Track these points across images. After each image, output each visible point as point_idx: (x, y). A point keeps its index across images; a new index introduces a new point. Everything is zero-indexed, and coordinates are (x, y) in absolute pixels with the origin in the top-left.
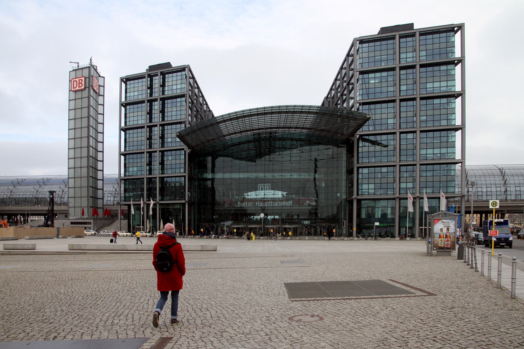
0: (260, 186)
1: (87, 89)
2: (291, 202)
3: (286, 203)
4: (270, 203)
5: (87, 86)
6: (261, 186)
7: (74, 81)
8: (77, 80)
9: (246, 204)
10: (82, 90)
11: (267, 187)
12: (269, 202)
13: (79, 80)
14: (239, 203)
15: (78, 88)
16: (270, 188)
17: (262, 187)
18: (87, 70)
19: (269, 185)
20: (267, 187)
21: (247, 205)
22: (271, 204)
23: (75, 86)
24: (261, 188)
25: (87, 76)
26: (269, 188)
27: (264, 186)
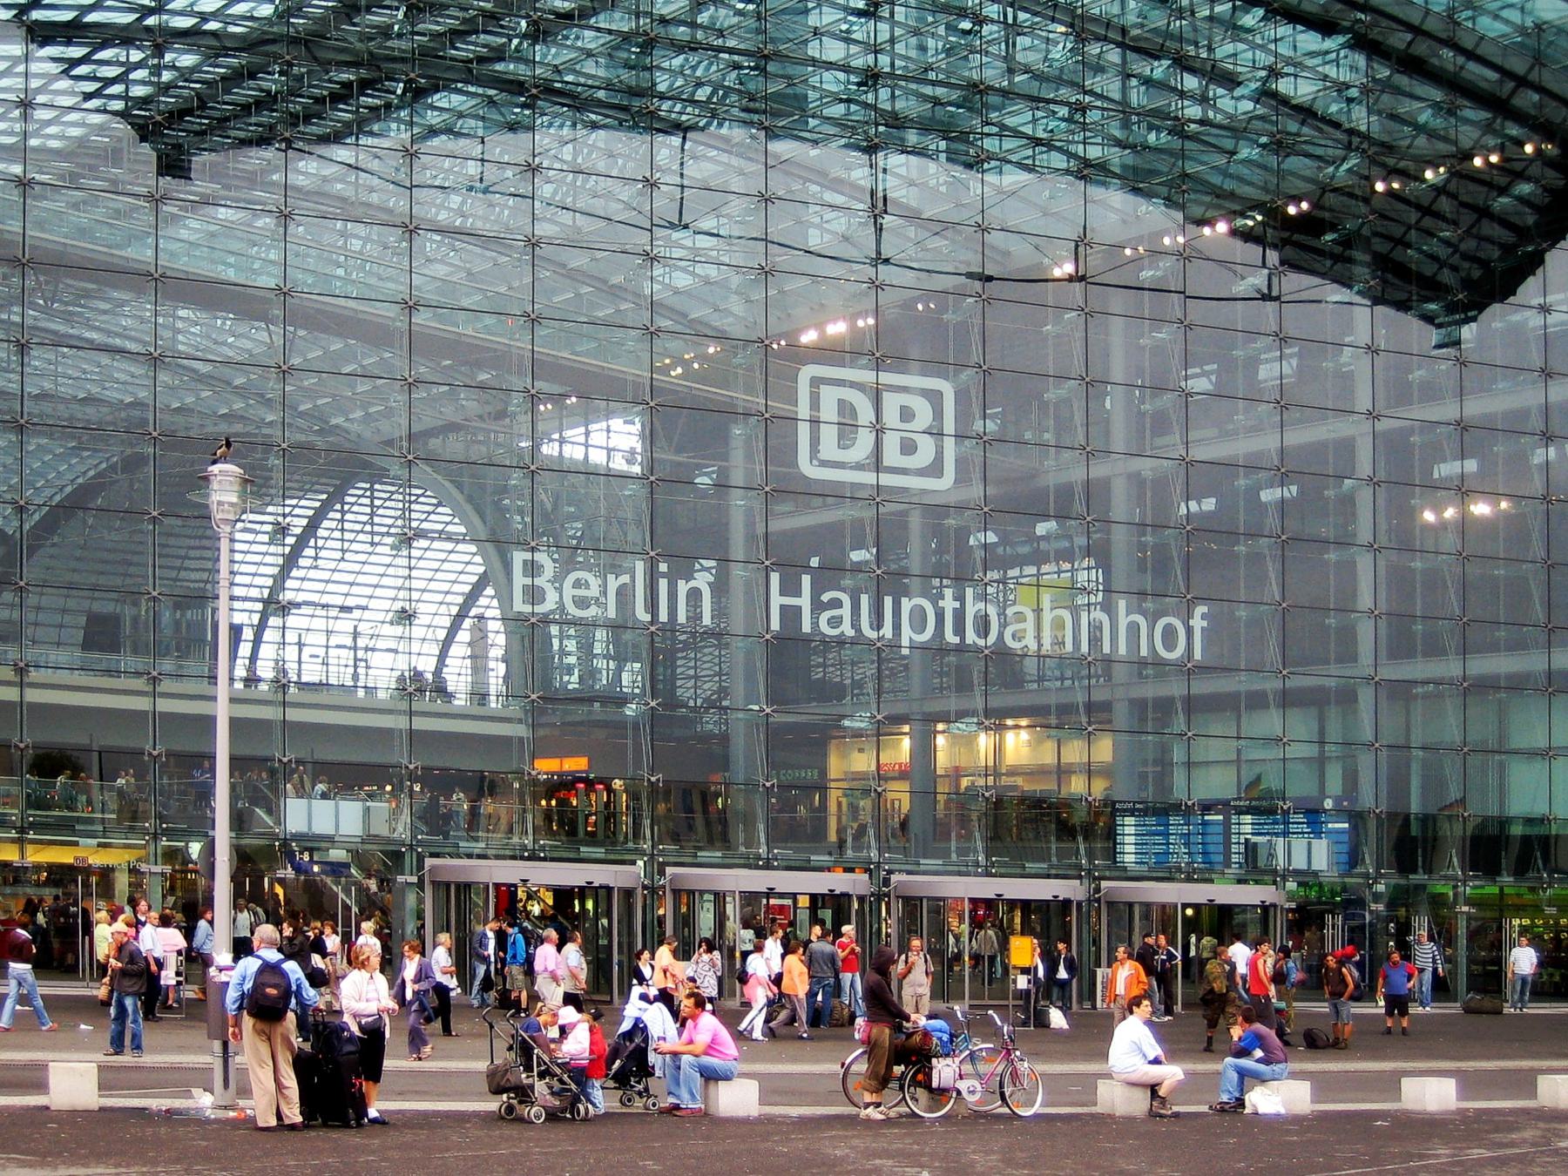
0: (816, 382)
2: (1198, 623)
3: (1134, 629)
4: (949, 604)
6: (829, 396)
11: (906, 414)
12: (936, 598)
14: (532, 569)
16: (949, 426)
17: (845, 408)
19: (935, 398)
20: (906, 414)
21: (652, 606)
22: (960, 616)
24: (829, 412)
26: (936, 433)
27: (877, 396)
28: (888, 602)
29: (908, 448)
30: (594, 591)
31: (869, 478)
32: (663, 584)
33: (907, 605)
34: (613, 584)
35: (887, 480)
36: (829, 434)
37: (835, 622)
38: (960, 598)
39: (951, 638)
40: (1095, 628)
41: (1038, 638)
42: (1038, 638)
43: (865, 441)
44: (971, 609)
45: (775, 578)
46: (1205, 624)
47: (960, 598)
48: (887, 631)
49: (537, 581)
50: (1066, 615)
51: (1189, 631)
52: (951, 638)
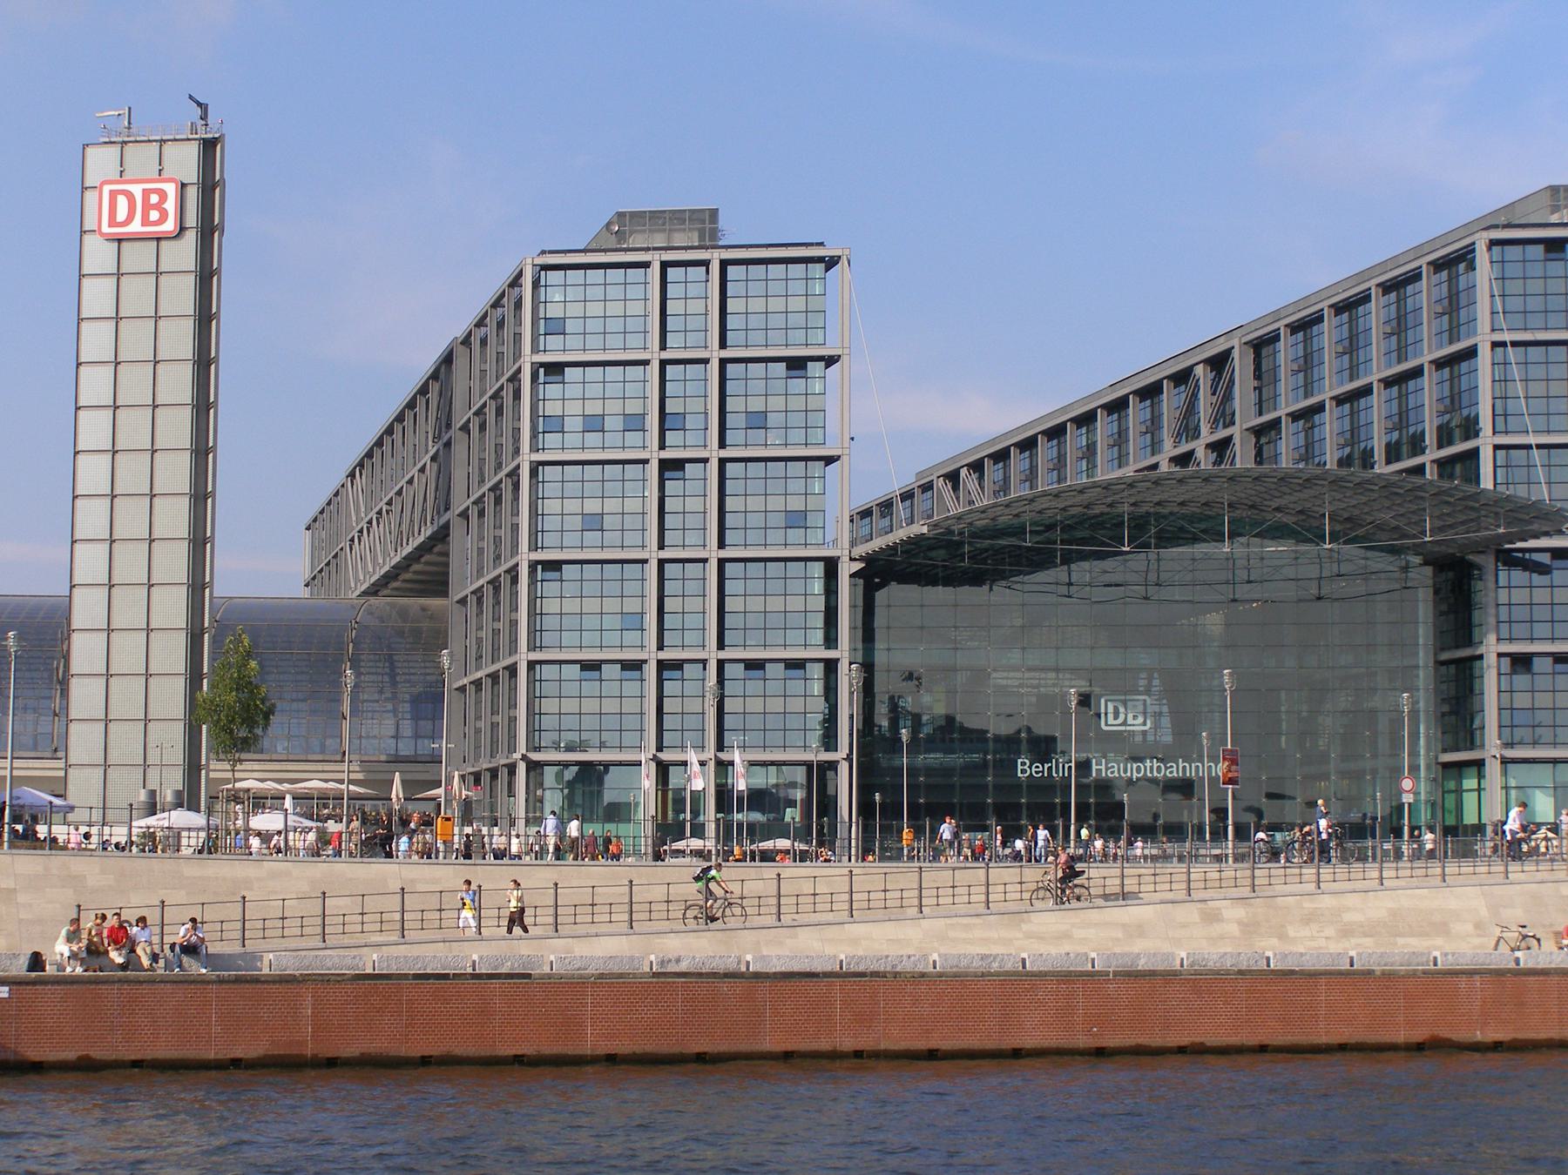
1: (191, 237)
4: (1148, 764)
5: (192, 219)
7: (113, 194)
8: (137, 190)
9: (1050, 769)
10: (158, 239)
13: (146, 193)
14: (1023, 764)
15: (136, 227)
17: (1116, 709)
18: (192, 152)
21: (1057, 772)
22: (1152, 768)
23: (122, 215)
25: (191, 174)
28: (1129, 765)
29: (1135, 717)
30: (1041, 769)
31: (1123, 728)
32: (1061, 765)
34: (1046, 766)
35: (1128, 728)
36: (1111, 716)
37: (1112, 773)
41: (1178, 772)
42: (1178, 772)
43: (1121, 719)
45: (1094, 761)
47: (1152, 762)
48: (1129, 774)
49: (1026, 767)
52: (1149, 775)
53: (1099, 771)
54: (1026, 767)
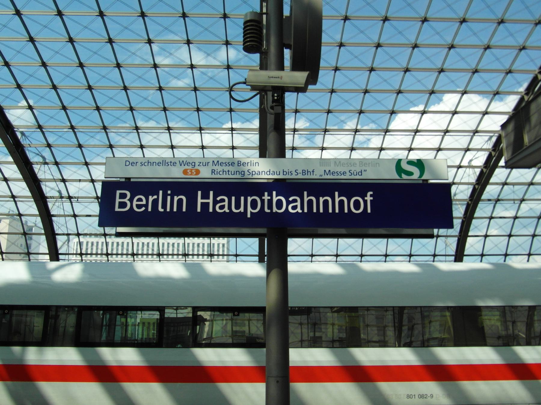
2: (369, 198)
3: (341, 203)
4: (266, 197)
12: (261, 196)
33: (249, 199)
37: (222, 207)
38: (270, 195)
39: (267, 210)
40: (326, 203)
41: (302, 208)
44: (275, 199)
46: (372, 198)
47: (270, 195)
48: (242, 209)
49: (126, 200)
50: (314, 199)
51: (365, 202)
53: (205, 206)
54: (126, 200)
